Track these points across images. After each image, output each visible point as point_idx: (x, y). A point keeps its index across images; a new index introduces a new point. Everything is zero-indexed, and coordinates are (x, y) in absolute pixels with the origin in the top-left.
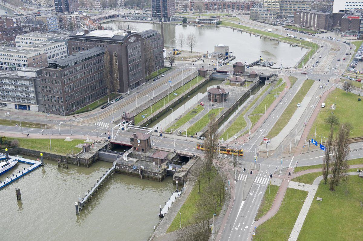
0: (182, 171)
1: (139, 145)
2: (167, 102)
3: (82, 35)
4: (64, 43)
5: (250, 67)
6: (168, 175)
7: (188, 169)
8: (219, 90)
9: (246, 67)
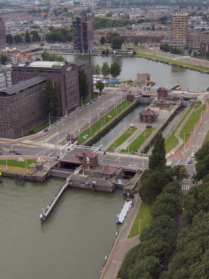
0: (131, 184)
1: (88, 163)
3: (23, 66)
4: (3, 74)
5: (171, 92)
6: (117, 188)
7: (136, 183)
8: (150, 112)
9: (168, 92)
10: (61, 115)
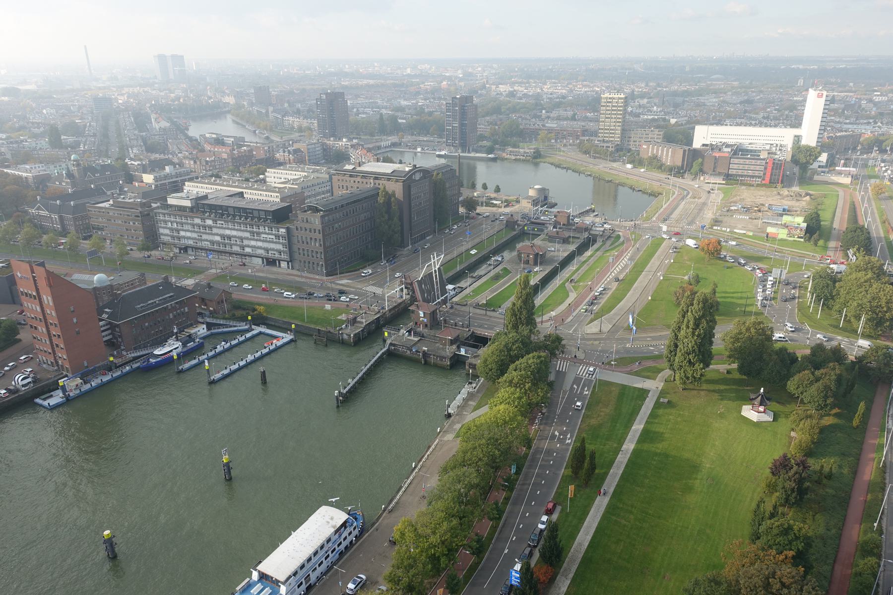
1: (421, 319)
2: (461, 263)
6: (457, 362)
10: (403, 245)
